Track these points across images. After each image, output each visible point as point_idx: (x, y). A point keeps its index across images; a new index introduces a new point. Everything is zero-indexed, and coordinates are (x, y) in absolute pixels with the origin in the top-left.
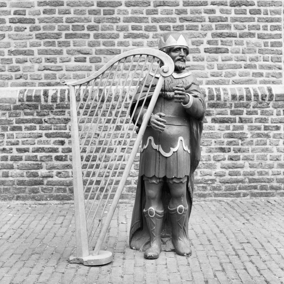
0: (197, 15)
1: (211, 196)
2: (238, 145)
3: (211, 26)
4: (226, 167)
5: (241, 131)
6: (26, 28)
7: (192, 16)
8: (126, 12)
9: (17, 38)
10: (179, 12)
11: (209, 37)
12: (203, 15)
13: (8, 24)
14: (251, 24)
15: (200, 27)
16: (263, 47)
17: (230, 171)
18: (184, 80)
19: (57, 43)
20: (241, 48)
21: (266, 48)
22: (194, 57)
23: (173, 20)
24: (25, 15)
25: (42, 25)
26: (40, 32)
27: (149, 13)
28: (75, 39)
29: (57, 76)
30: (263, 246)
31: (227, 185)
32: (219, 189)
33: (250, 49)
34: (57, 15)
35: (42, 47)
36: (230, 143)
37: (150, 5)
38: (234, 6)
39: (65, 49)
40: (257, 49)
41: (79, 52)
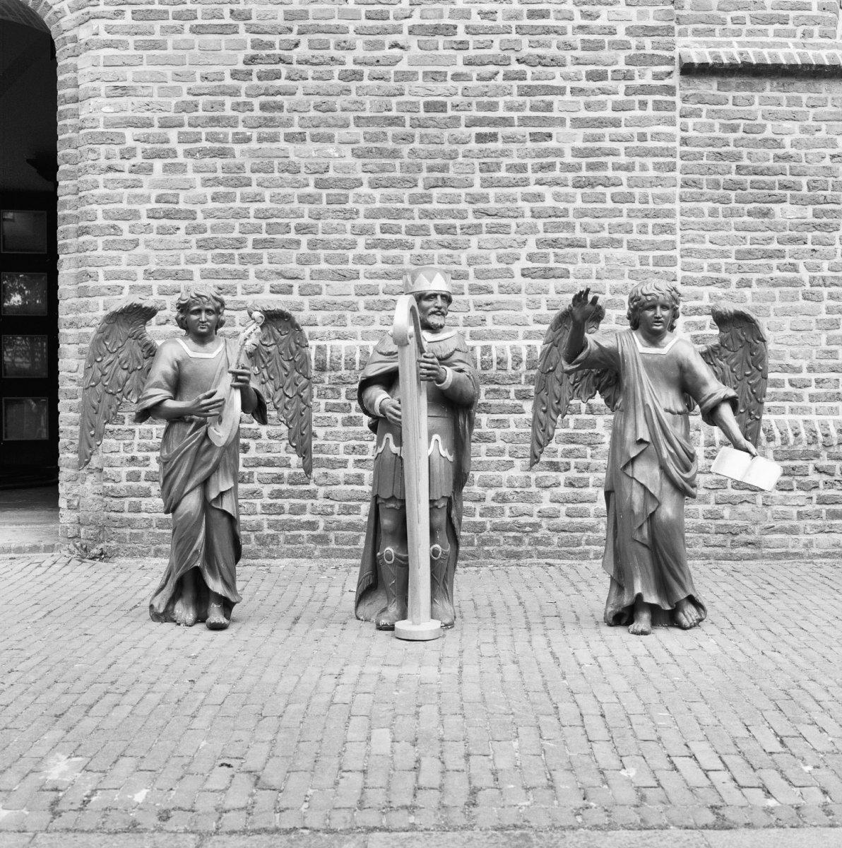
0: (508, 204)
1: (531, 557)
2: (585, 457)
3: (536, 226)
4: (561, 500)
5: (591, 431)
6: (178, 229)
7: (499, 206)
8: (371, 199)
9: (160, 247)
10: (473, 199)
11: (531, 247)
12: (520, 203)
13: (145, 221)
14: (615, 221)
15: (514, 227)
16: (638, 267)
17: (568, 509)
18: (442, 344)
19: (237, 257)
20: (594, 267)
21: (644, 268)
22: (501, 286)
23: (461, 215)
24: (177, 203)
25: (209, 222)
26: (206, 235)
27: (414, 200)
28: (271, 251)
29: (237, 321)
30: (578, 619)
31: (563, 534)
32: (547, 542)
33: (611, 271)
34: (237, 204)
35: (210, 265)
36: (568, 454)
37: (416, 186)
38: (581, 187)
39: (252, 269)
40: (626, 270)
41: (280, 274)
